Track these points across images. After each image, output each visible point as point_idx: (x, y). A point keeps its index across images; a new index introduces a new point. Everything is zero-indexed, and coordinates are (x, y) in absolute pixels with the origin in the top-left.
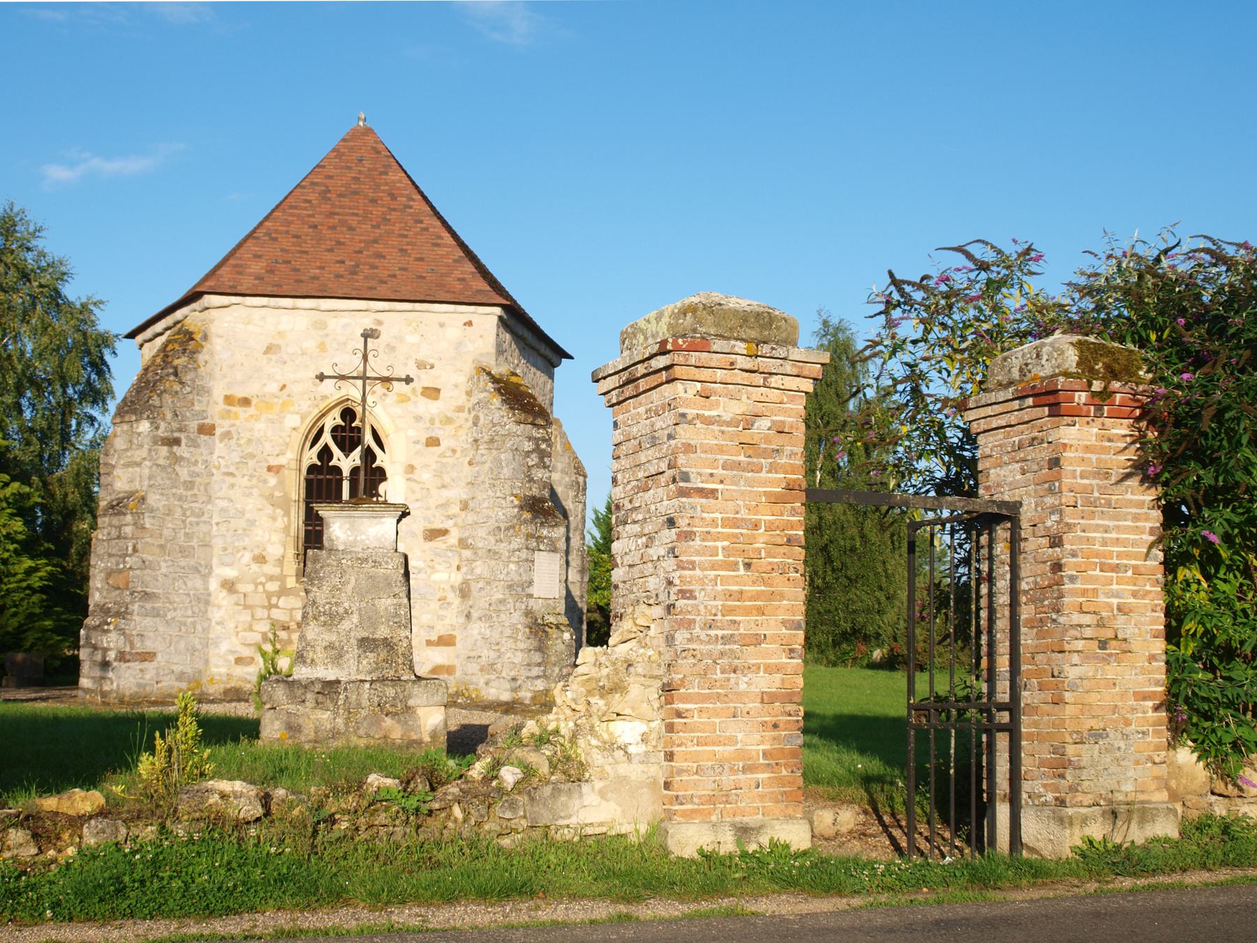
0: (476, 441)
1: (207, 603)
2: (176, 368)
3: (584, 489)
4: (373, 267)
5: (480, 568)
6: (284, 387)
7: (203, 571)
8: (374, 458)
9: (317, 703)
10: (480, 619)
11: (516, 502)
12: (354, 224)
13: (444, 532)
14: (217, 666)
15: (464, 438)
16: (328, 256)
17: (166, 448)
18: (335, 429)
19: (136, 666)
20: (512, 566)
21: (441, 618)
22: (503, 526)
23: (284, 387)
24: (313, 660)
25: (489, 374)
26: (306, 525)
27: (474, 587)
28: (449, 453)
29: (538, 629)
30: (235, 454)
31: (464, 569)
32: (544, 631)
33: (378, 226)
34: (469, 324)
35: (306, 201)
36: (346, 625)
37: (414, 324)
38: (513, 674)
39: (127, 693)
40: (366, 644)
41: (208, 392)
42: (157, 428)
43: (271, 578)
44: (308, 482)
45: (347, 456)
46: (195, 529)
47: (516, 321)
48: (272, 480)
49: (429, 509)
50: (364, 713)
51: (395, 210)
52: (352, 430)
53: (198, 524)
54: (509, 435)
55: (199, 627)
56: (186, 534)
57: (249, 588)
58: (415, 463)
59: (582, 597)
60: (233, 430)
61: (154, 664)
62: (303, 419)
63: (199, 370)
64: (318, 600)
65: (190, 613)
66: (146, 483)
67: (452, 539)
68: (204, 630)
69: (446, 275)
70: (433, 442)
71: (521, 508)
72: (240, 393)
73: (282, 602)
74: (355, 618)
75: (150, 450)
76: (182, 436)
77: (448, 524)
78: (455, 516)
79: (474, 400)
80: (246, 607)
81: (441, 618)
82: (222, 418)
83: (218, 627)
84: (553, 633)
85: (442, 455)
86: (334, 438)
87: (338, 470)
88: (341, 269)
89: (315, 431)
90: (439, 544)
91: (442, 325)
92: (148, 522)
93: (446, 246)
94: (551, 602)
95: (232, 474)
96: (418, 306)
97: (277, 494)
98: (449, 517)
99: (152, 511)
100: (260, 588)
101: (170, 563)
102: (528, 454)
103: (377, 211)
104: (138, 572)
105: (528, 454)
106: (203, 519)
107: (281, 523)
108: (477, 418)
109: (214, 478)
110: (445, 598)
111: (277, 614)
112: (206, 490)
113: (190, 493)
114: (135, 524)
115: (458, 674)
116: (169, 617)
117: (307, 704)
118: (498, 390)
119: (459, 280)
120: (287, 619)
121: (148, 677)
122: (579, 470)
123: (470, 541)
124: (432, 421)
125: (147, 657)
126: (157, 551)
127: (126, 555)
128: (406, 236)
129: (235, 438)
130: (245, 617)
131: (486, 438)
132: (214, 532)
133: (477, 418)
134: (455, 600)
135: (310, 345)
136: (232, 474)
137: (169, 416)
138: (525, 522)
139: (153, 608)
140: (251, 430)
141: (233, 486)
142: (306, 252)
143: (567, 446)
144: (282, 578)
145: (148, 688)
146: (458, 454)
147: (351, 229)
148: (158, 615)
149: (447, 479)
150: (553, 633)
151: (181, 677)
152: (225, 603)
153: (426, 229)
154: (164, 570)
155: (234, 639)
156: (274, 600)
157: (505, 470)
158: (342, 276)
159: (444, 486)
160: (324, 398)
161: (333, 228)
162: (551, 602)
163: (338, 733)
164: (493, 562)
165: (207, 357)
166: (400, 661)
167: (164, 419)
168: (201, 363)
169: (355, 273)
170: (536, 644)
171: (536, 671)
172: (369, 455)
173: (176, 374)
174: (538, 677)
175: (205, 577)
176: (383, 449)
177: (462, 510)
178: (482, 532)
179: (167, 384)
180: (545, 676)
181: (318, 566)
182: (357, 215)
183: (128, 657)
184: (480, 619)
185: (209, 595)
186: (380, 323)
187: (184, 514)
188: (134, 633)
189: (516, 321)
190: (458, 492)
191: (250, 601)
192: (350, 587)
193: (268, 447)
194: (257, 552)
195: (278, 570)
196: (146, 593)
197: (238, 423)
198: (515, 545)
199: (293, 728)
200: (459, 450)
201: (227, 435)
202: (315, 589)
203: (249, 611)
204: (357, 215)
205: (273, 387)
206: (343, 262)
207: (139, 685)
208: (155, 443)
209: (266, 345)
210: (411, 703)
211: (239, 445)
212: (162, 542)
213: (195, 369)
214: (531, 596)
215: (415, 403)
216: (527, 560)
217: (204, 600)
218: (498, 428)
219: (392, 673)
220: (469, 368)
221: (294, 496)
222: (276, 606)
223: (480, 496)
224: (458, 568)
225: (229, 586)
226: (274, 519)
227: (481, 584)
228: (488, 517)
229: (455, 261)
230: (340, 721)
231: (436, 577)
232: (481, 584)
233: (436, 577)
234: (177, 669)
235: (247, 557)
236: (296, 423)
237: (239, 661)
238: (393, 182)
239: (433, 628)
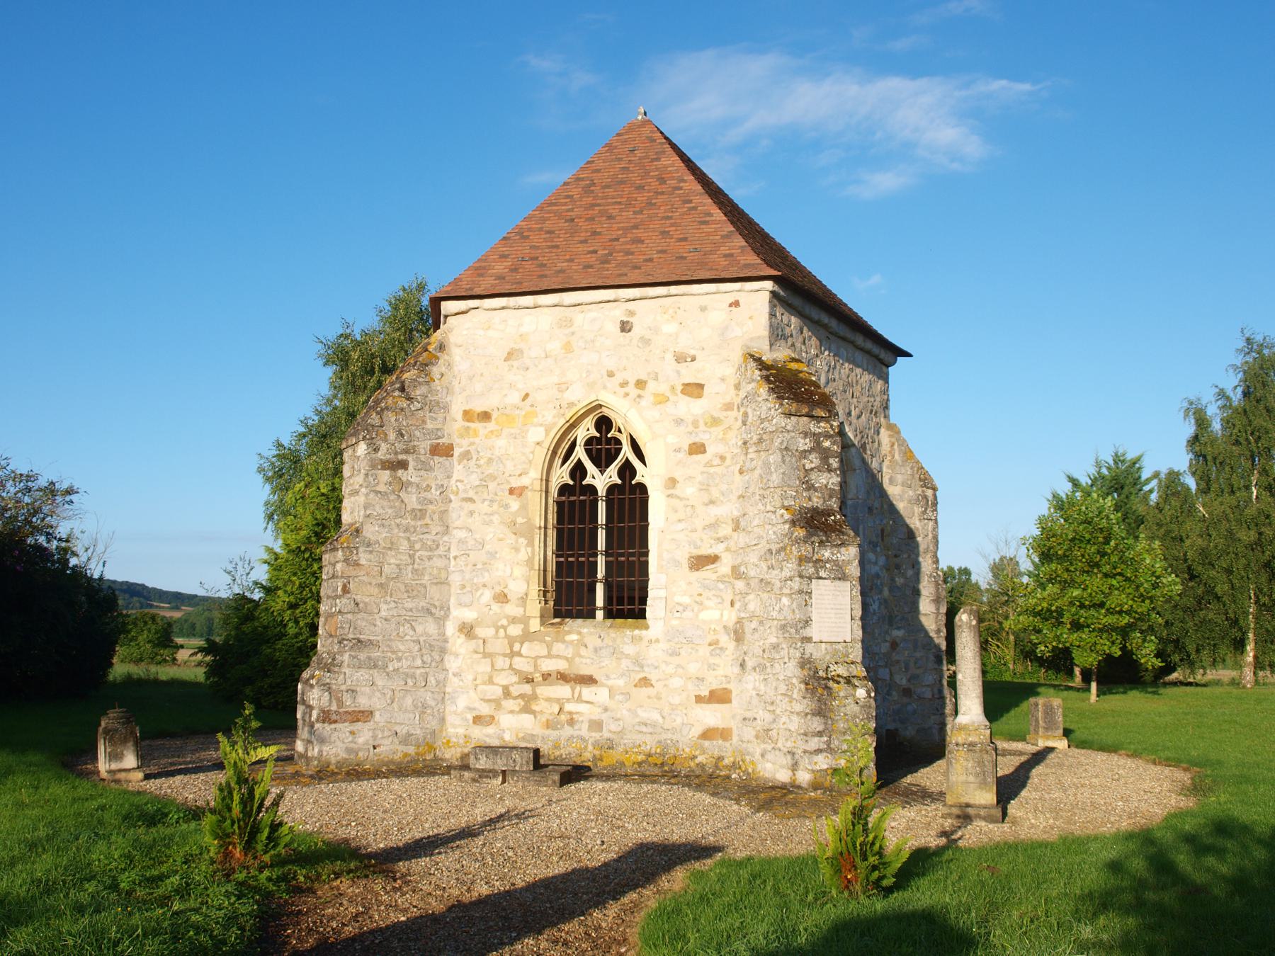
0: (745, 443)
1: (443, 651)
2: (403, 383)
3: (935, 504)
4: (628, 253)
5: (753, 604)
6: (527, 395)
7: (438, 613)
8: (633, 472)
10: (754, 669)
11: (787, 516)
12: (614, 212)
13: (714, 559)
14: (454, 726)
15: (734, 441)
16: (581, 248)
17: (388, 472)
18: (589, 442)
19: (345, 727)
20: (785, 600)
21: (712, 667)
22: (774, 547)
23: (527, 395)
25: (758, 360)
26: (557, 556)
27: (749, 627)
28: (717, 461)
29: (819, 684)
30: (474, 476)
31: (737, 605)
32: (827, 687)
33: (641, 212)
34: (736, 304)
35: (568, 197)
37: (671, 311)
38: (789, 744)
39: (333, 760)
41: (446, 408)
42: (376, 450)
43: (514, 620)
44: (560, 505)
45: (602, 472)
46: (427, 564)
47: (801, 295)
48: (514, 504)
49: (694, 531)
51: (663, 193)
52: (609, 441)
53: (430, 558)
54: (776, 431)
55: (432, 680)
56: (415, 571)
57: (490, 632)
58: (677, 475)
59: (939, 631)
60: (472, 449)
61: (371, 725)
62: (547, 432)
63: (432, 384)
65: (419, 662)
66: (362, 513)
67: (724, 567)
68: (438, 683)
69: (711, 252)
70: (697, 449)
71: (793, 523)
72: (479, 408)
73: (526, 649)
75: (367, 475)
76: (411, 460)
77: (718, 549)
78: (726, 538)
79: (743, 394)
80: (486, 655)
81: (712, 667)
82: (461, 436)
83: (456, 680)
84: (841, 690)
85: (709, 464)
86: (588, 452)
87: (592, 489)
88: (592, 259)
89: (565, 446)
90: (707, 573)
91: (703, 309)
92: (363, 558)
93: (715, 222)
94: (839, 647)
95: (471, 500)
96: (673, 289)
97: (520, 520)
98: (720, 540)
99: (369, 545)
100: (502, 631)
101: (393, 605)
102: (804, 454)
103: (642, 197)
104: (349, 616)
105: (804, 454)
106: (436, 553)
107: (523, 555)
108: (746, 415)
109: (452, 505)
110: (717, 642)
111: (519, 663)
112: (441, 519)
113: (419, 523)
114: (346, 560)
115: (735, 739)
116: (391, 668)
118: (767, 379)
119: (725, 256)
120: (531, 669)
121: (361, 740)
122: (926, 481)
123: (743, 569)
124: (695, 424)
125: (362, 716)
126: (375, 591)
127: (337, 597)
128: (671, 218)
129: (475, 458)
130: (484, 667)
131: (755, 438)
132: (452, 569)
133: (746, 415)
134: (727, 641)
135: (555, 346)
136: (471, 500)
137: (392, 436)
138: (797, 541)
139: (369, 658)
140: (492, 448)
141: (471, 513)
142: (557, 247)
143: (908, 455)
144: (524, 620)
145: (361, 754)
146: (728, 462)
147: (610, 217)
148: (375, 666)
149: (715, 493)
150: (841, 690)
151: (406, 740)
152: (462, 651)
153: (695, 208)
154: (383, 614)
155: (472, 693)
156: (517, 647)
157: (774, 477)
158: (591, 267)
159: (712, 502)
160: (571, 405)
161: (592, 219)
162: (839, 647)
164: (765, 595)
165: (443, 369)
167: (385, 440)
168: (436, 375)
169: (607, 262)
171: (815, 743)
172: (627, 471)
173: (402, 389)
175: (441, 621)
176: (643, 461)
177: (734, 530)
178: (753, 558)
179: (390, 400)
180: (829, 749)
182: (620, 203)
183: (334, 717)
184: (754, 669)
185: (446, 641)
186: (632, 313)
187: (412, 548)
188: (344, 688)
189: (801, 295)
190: (729, 509)
191: (490, 649)
193: (509, 464)
194: (498, 589)
195: (521, 610)
196: (359, 641)
197: (477, 440)
198: (787, 573)
200: (728, 456)
201: (466, 455)
203: (488, 660)
204: (620, 203)
205: (515, 398)
206: (596, 252)
207: (348, 750)
208: (373, 467)
209: (507, 350)
211: (479, 466)
212: (383, 580)
213: (427, 383)
214: (809, 640)
215: (675, 403)
216: (800, 592)
217: (440, 648)
218: (766, 424)
220: (737, 356)
221: (538, 521)
222: (519, 654)
223: (752, 511)
224: (732, 604)
225: (468, 630)
226: (517, 550)
227: (754, 625)
228: (760, 537)
229: (722, 237)
231: (705, 615)
232: (754, 625)
233: (705, 615)
234: (402, 730)
235: (487, 596)
236: (540, 436)
237: (478, 720)
238: (666, 167)
239: (703, 680)
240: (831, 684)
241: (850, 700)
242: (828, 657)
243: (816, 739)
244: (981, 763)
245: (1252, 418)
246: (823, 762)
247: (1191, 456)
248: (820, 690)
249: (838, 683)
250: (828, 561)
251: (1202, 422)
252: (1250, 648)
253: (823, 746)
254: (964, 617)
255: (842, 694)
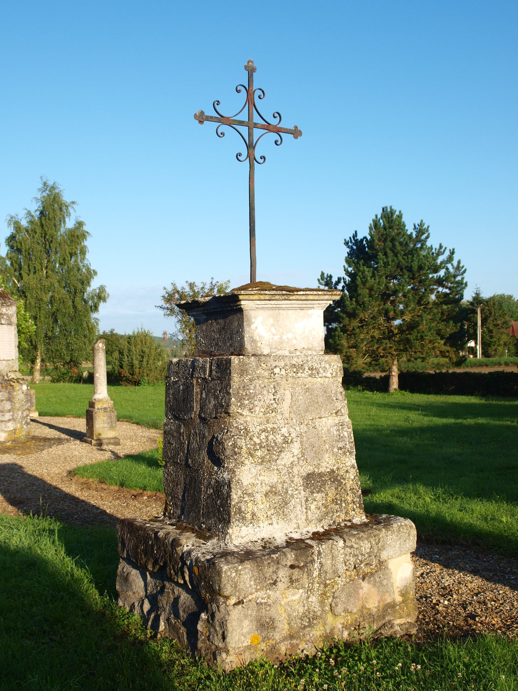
9: (292, 581)
24: (253, 514)
32: (11, 385)
36: (286, 458)
40: (313, 481)
50: (341, 582)
64: (251, 428)
74: (296, 448)
117: (279, 584)
162: (10, 362)
163: (315, 618)
166: (349, 499)
170: (6, 395)
171: (8, 416)
174: (9, 420)
180: (13, 419)
181: (246, 379)
192: (285, 406)
199: (266, 625)
202: (246, 412)
210: (384, 555)
219: (343, 516)
230: (313, 599)
240: (12, 383)
241: (20, 392)
242: (6, 369)
243: (8, 414)
244: (110, 417)
245: (46, 229)
246: (11, 426)
247: (8, 248)
248: (9, 387)
249: (14, 382)
250: (5, 314)
251: (18, 227)
252: (38, 361)
253: (11, 418)
254: (100, 345)
255: (17, 388)
